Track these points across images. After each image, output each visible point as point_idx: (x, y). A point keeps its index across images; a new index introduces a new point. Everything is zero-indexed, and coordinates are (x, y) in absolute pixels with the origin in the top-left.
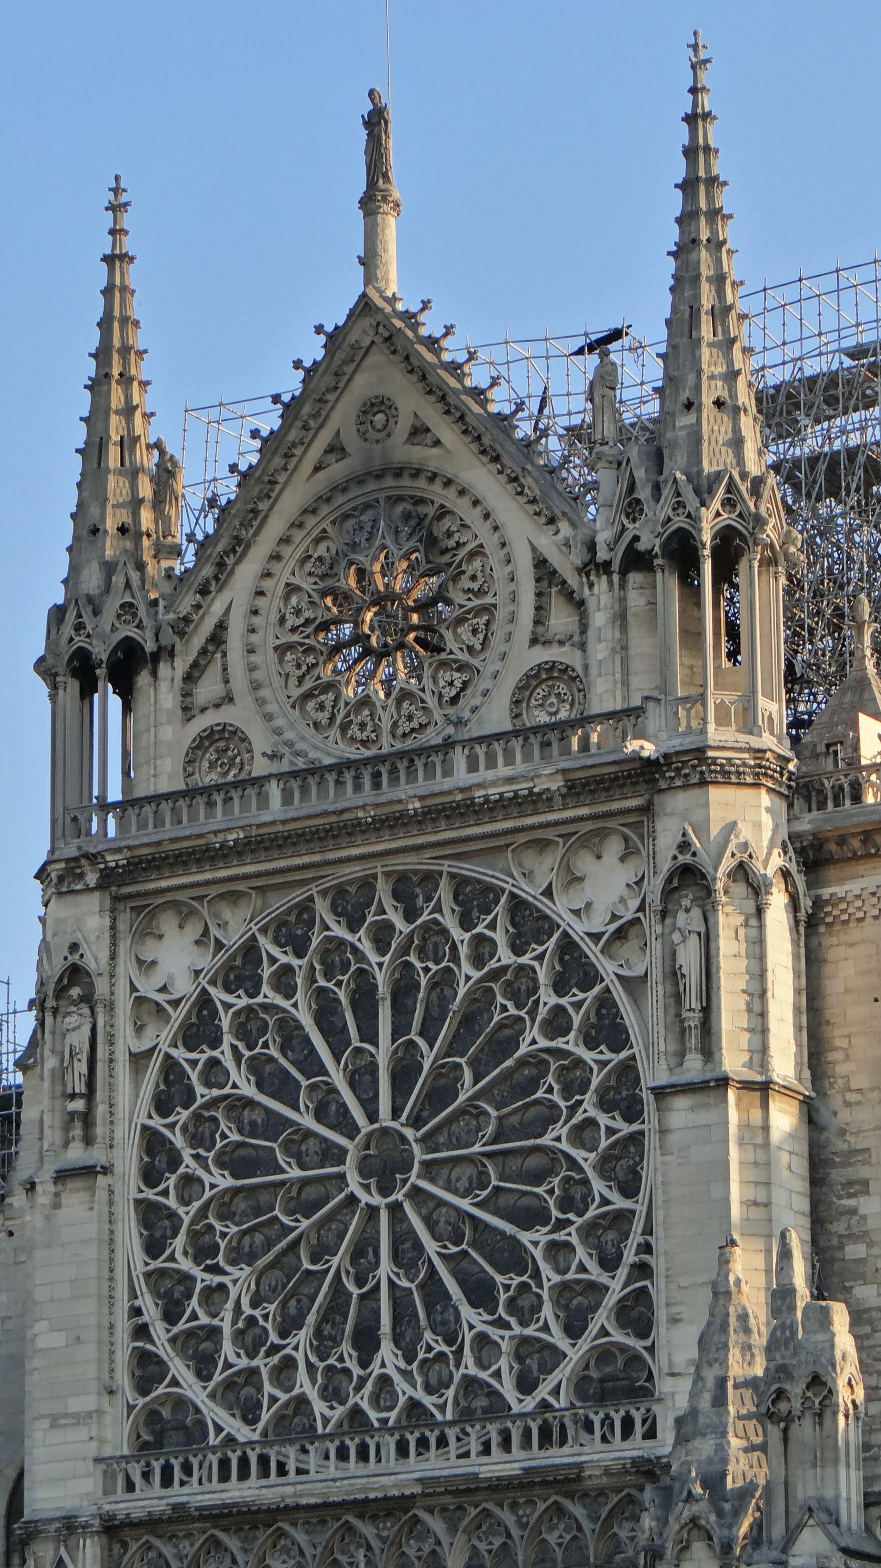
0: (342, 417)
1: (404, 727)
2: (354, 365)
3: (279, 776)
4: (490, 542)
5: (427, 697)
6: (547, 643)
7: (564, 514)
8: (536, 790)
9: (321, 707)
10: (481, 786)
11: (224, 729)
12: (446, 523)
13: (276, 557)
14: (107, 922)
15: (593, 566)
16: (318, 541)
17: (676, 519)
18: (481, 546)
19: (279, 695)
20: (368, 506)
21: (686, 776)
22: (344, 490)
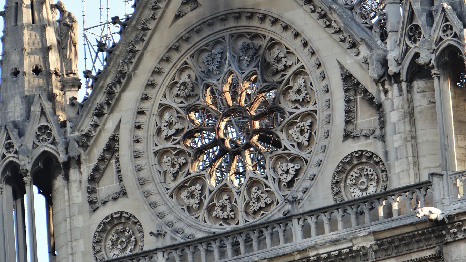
1: (254, 206)
3: (164, 249)
6: (356, 137)
7: (362, 40)
8: (355, 248)
9: (192, 195)
10: (313, 247)
11: (121, 216)
12: (276, 51)
13: (151, 85)
15: (386, 78)
17: (446, 38)
18: (303, 67)
19: (159, 188)
20: (217, 42)
22: (198, 32)
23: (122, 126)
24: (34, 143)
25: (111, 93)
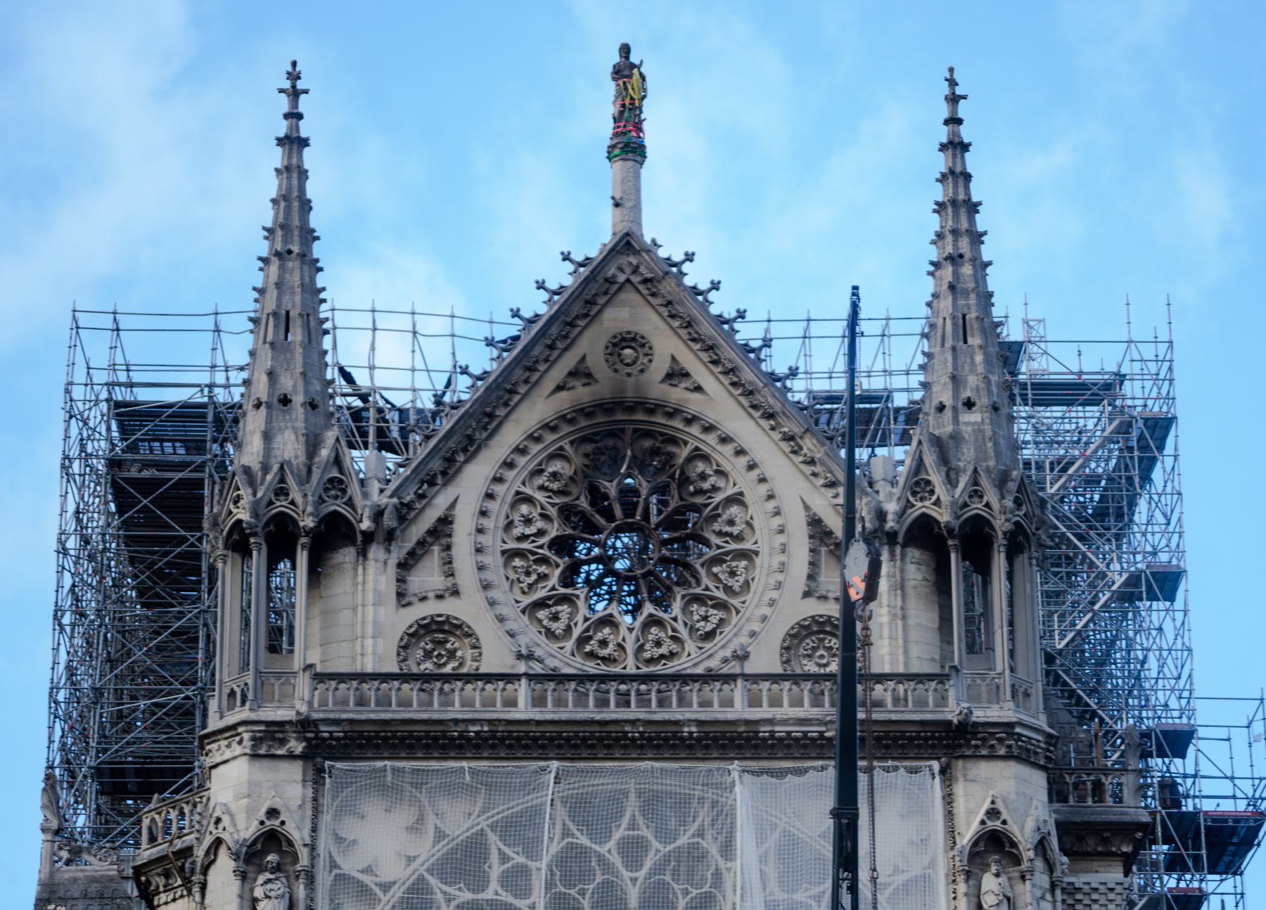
0: (591, 344)
2: (607, 297)
3: (531, 677)
4: (754, 494)
5: (680, 626)
9: (555, 617)
12: (700, 466)
13: (509, 465)
14: (310, 793)
16: (551, 457)
21: (992, 746)
23: (459, 506)
24: (320, 497)
25: (450, 460)
